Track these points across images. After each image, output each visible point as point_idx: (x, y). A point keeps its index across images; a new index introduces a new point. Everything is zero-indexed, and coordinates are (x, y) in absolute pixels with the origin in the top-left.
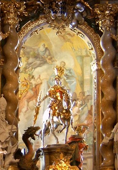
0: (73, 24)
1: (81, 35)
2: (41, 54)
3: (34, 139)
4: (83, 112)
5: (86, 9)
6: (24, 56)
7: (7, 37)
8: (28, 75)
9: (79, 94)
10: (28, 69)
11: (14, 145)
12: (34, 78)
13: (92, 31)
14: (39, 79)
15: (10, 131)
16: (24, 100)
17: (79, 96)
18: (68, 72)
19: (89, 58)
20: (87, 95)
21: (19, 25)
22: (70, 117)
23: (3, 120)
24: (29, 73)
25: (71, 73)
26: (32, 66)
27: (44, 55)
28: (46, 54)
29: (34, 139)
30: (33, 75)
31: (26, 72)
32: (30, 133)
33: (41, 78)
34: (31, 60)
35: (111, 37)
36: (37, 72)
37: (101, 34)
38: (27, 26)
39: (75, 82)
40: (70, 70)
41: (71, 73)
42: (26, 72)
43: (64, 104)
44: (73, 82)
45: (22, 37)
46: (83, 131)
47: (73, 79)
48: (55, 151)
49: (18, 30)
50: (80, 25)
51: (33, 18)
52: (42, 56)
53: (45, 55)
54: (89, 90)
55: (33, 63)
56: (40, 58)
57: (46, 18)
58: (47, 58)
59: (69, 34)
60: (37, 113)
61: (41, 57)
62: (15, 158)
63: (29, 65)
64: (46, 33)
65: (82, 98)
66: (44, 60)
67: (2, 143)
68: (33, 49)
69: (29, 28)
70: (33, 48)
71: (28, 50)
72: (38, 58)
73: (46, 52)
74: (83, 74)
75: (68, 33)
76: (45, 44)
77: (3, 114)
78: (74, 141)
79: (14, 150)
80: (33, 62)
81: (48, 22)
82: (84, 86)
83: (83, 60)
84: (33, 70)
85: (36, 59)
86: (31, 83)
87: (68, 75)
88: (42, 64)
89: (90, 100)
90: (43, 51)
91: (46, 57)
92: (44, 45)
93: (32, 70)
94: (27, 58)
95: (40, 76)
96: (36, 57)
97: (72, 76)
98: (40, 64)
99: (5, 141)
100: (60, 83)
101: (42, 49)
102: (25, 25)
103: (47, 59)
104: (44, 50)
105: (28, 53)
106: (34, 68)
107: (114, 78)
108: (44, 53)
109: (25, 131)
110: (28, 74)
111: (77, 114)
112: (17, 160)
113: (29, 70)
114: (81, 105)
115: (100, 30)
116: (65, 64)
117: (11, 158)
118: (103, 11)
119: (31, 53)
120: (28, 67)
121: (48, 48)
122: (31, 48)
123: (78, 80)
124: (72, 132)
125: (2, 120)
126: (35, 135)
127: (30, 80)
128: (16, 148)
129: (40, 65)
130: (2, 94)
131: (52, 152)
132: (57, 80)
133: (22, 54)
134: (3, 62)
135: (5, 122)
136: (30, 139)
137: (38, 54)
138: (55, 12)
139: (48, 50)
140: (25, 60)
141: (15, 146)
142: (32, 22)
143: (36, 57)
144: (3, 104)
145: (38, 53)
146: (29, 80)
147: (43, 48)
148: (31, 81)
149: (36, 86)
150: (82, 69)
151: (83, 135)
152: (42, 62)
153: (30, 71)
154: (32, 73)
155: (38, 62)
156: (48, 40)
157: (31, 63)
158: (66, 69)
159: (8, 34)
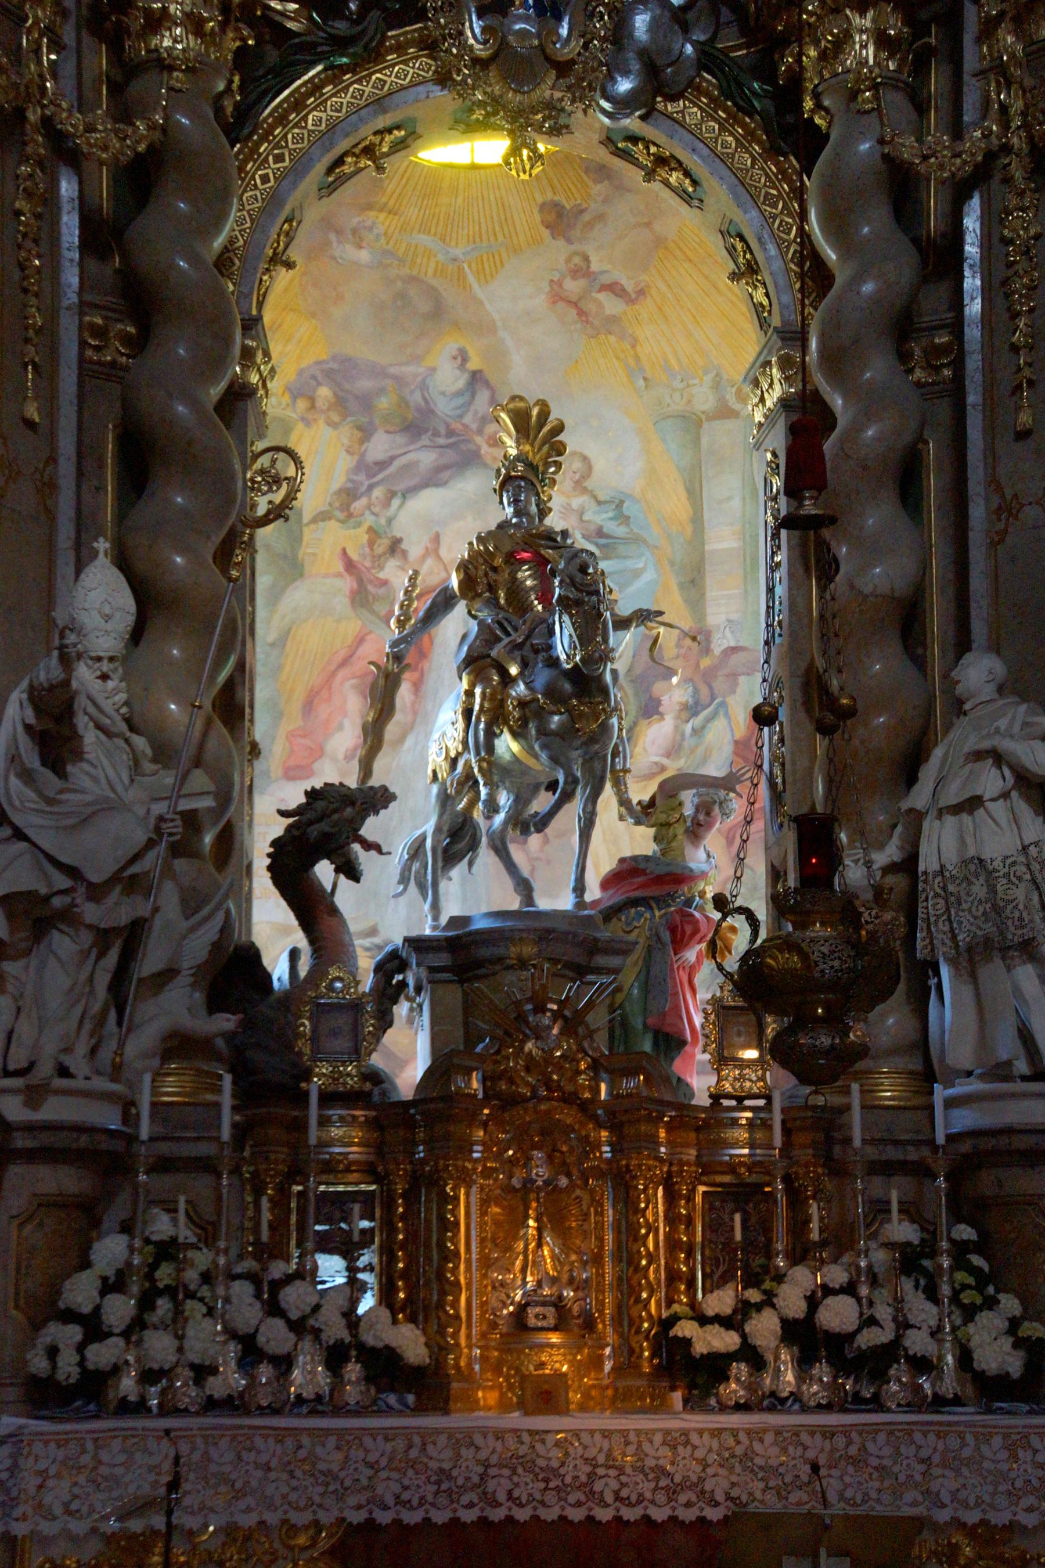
0: (624, 86)
1: (674, 178)
2: (444, 407)
3: (350, 871)
4: (700, 751)
6: (336, 418)
7: (141, 148)
8: (366, 537)
9: (678, 646)
10: (363, 501)
11: (196, 911)
12: (404, 554)
13: (750, 135)
14: (430, 562)
15: (159, 808)
16: (342, 683)
17: (678, 657)
18: (611, 514)
19: (730, 424)
20: (725, 644)
21: (237, 79)
22: (605, 728)
23: (107, 721)
24: (369, 520)
25: (625, 520)
26: (383, 480)
27: (461, 416)
28: (472, 408)
29: (350, 871)
30: (399, 535)
31: (349, 517)
32: (329, 828)
33: (443, 552)
34: (380, 446)
35: (886, 157)
38: (297, 104)
39: (649, 576)
40: (622, 502)
41: (625, 520)
42: (350, 515)
43: (563, 640)
44: (637, 574)
45: (265, 179)
46: (696, 831)
47: (641, 555)
48: (500, 951)
49: (239, 125)
50: (673, 98)
51: (340, 44)
52: (448, 425)
53: (468, 419)
54: (734, 617)
55: (397, 464)
56: (436, 434)
57: (430, 46)
58: (480, 431)
59: (614, 288)
61: (443, 430)
62: (214, 1005)
63: (370, 476)
64: (476, 286)
65: (698, 665)
66: (463, 447)
67: (90, 884)
68: (395, 378)
70: (393, 370)
71: (365, 384)
72: (426, 431)
73: (473, 395)
74: (697, 520)
75: (606, 279)
76: (472, 353)
77: (111, 684)
78: (638, 894)
80: (393, 458)
81: (443, 79)
82: (703, 594)
83: (697, 440)
84: (396, 502)
85: (412, 442)
86: (385, 583)
87: (605, 530)
88: (447, 467)
89: (742, 679)
90: (458, 394)
91: (474, 426)
92: (462, 357)
93: (387, 504)
94: (358, 434)
95: (437, 539)
96: (416, 425)
97: (636, 540)
98: (439, 469)
99: (115, 878)
100: (534, 509)
101: (448, 378)
102: (286, 93)
103: (478, 439)
104: (461, 383)
105: (366, 402)
106: (404, 496)
107: (907, 438)
108: (460, 401)
109: (283, 813)
110: (365, 527)
111: (665, 761)
112: (226, 1022)
113: (369, 507)
114: (691, 709)
115: (811, 120)
116: (590, 468)
117: (178, 1007)
119: (384, 403)
120: (363, 489)
121: (491, 376)
122: (379, 372)
123: (672, 563)
124: (620, 839)
125: (99, 727)
126: (356, 847)
127: (378, 561)
128: (209, 933)
129: (434, 479)
130: (101, 539)
131: (480, 964)
132: (520, 487)
133: (328, 409)
134: (126, 339)
135: (127, 741)
136: (324, 871)
137: (427, 411)
139: (487, 384)
140: (346, 441)
141: (207, 919)
142: (335, 74)
143: (416, 425)
144: (107, 610)
145: (423, 403)
146: (368, 564)
147: (458, 372)
148: (381, 568)
150: (694, 494)
151: (696, 858)
152: (451, 456)
153: (376, 510)
154: (390, 521)
155: (427, 459)
156: (484, 327)
157: (382, 465)
158: (595, 497)
159: (152, 127)
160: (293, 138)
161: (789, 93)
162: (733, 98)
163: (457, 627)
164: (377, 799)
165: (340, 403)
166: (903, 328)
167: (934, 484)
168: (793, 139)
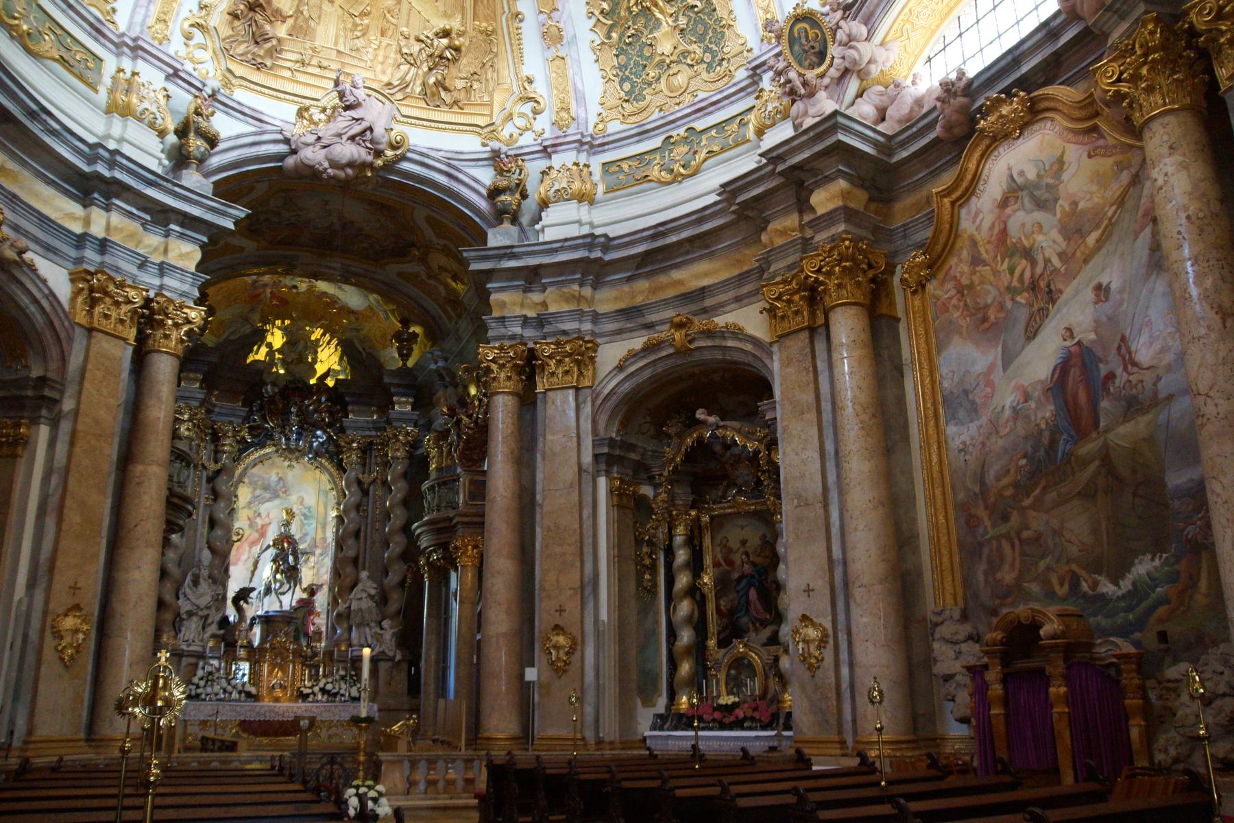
2: (273, 485)
5: (330, 438)
34: (258, 492)
36: (264, 508)
37: (345, 471)
43: (291, 558)
49: (237, 459)
60: (255, 567)
69: (252, 457)
79: (218, 617)
96: (266, 488)
101: (274, 478)
105: (256, 483)
118: (350, 444)
129: (269, 500)
138: (288, 439)
149: (263, 526)
155: (268, 495)
160: (248, 461)
161: (342, 460)
162: (331, 459)
163: (272, 552)
164: (253, 589)
165: (250, 483)
166: (358, 507)
167: (362, 534)
168: (341, 468)
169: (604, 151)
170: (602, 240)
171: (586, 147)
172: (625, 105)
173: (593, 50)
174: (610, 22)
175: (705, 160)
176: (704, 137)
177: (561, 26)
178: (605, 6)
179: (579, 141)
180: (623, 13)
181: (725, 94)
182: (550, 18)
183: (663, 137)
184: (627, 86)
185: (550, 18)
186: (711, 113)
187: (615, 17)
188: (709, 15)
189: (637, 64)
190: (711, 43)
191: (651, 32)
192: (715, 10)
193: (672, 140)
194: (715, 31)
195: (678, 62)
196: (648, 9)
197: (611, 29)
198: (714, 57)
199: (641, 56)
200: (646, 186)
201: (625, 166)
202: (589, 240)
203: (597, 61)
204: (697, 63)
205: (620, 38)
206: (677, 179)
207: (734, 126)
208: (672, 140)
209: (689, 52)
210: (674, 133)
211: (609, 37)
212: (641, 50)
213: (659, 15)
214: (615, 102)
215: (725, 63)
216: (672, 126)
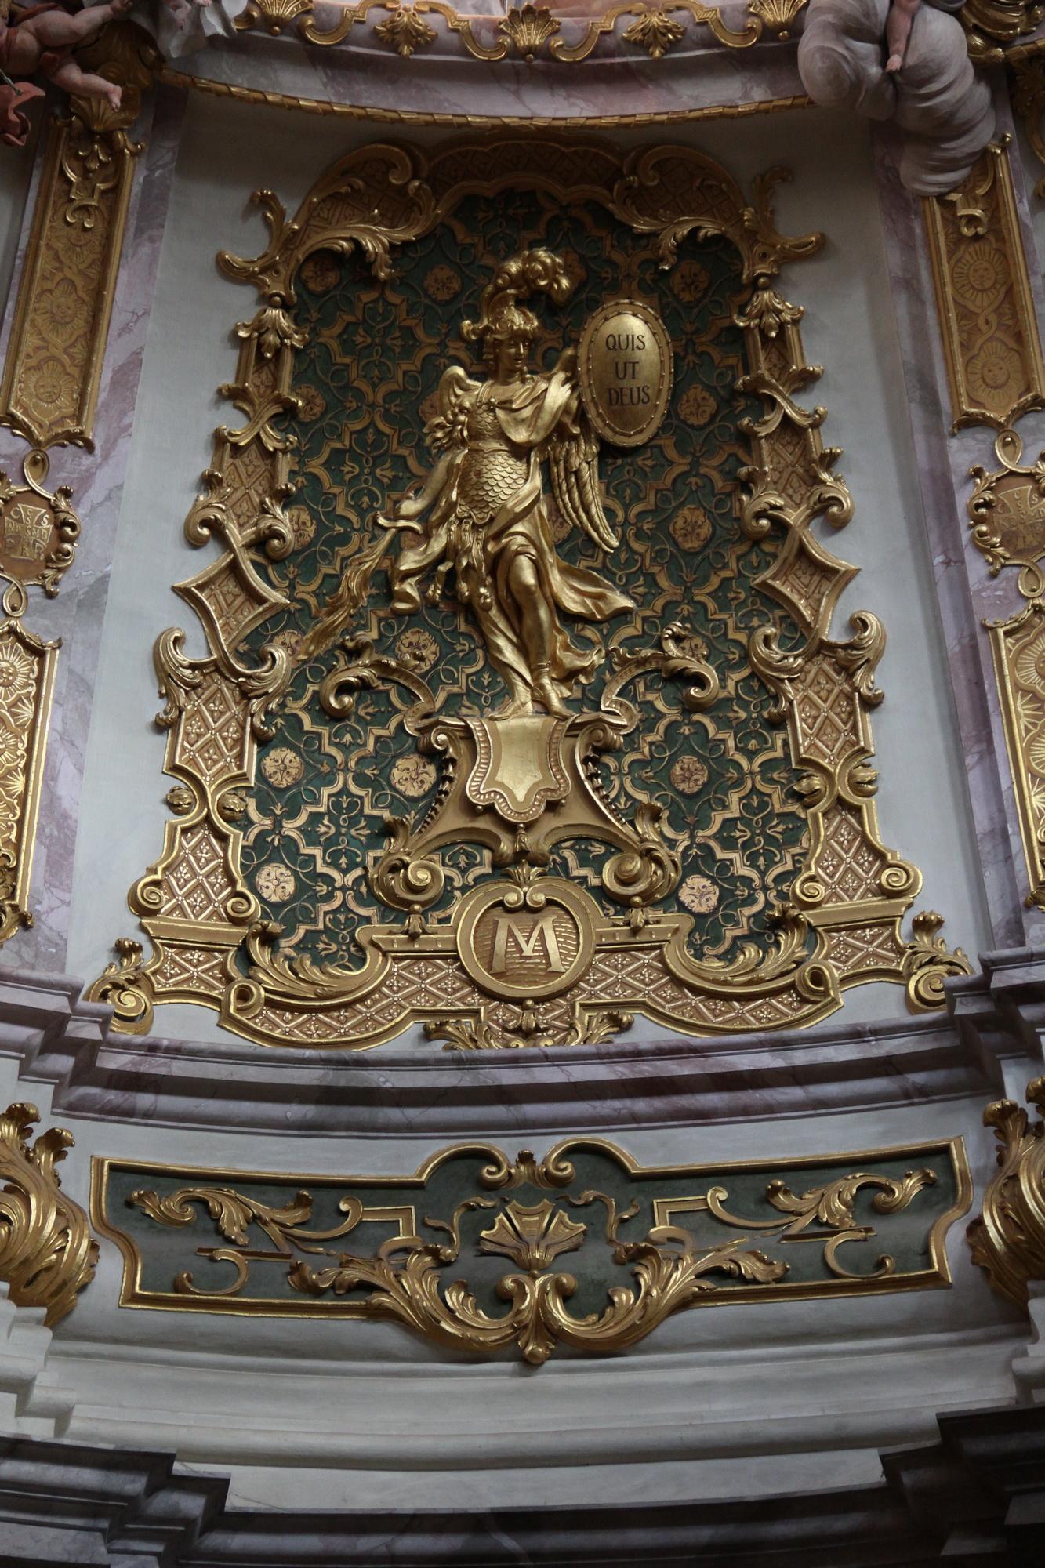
169: (124, 1114)
170: (193, 1505)
171: (64, 1063)
172: (260, 954)
173: (164, 674)
174: (276, 597)
175: (684, 1303)
176: (662, 1207)
177: (78, 514)
178: (283, 520)
179: (52, 1024)
180: (352, 582)
181: (800, 1057)
182: (40, 463)
183: (441, 1147)
184: (277, 882)
185: (40, 463)
186: (703, 1117)
187: (305, 591)
188: (742, 730)
189: (345, 808)
190: (728, 843)
191: (452, 704)
192: (779, 723)
193: (488, 1172)
194: (756, 804)
195: (550, 866)
196: (471, 611)
197: (279, 619)
198: (728, 900)
199: (379, 784)
200: (349, 1328)
201: (230, 1212)
202: (133, 1484)
203: (161, 727)
204: (649, 899)
205: (298, 680)
206: (533, 1345)
207: (837, 1199)
208: (488, 1172)
209: (615, 845)
210: (506, 1148)
211: (258, 658)
212: (384, 758)
213: (510, 656)
214: (202, 923)
215: (790, 944)
216: (498, 1112)
